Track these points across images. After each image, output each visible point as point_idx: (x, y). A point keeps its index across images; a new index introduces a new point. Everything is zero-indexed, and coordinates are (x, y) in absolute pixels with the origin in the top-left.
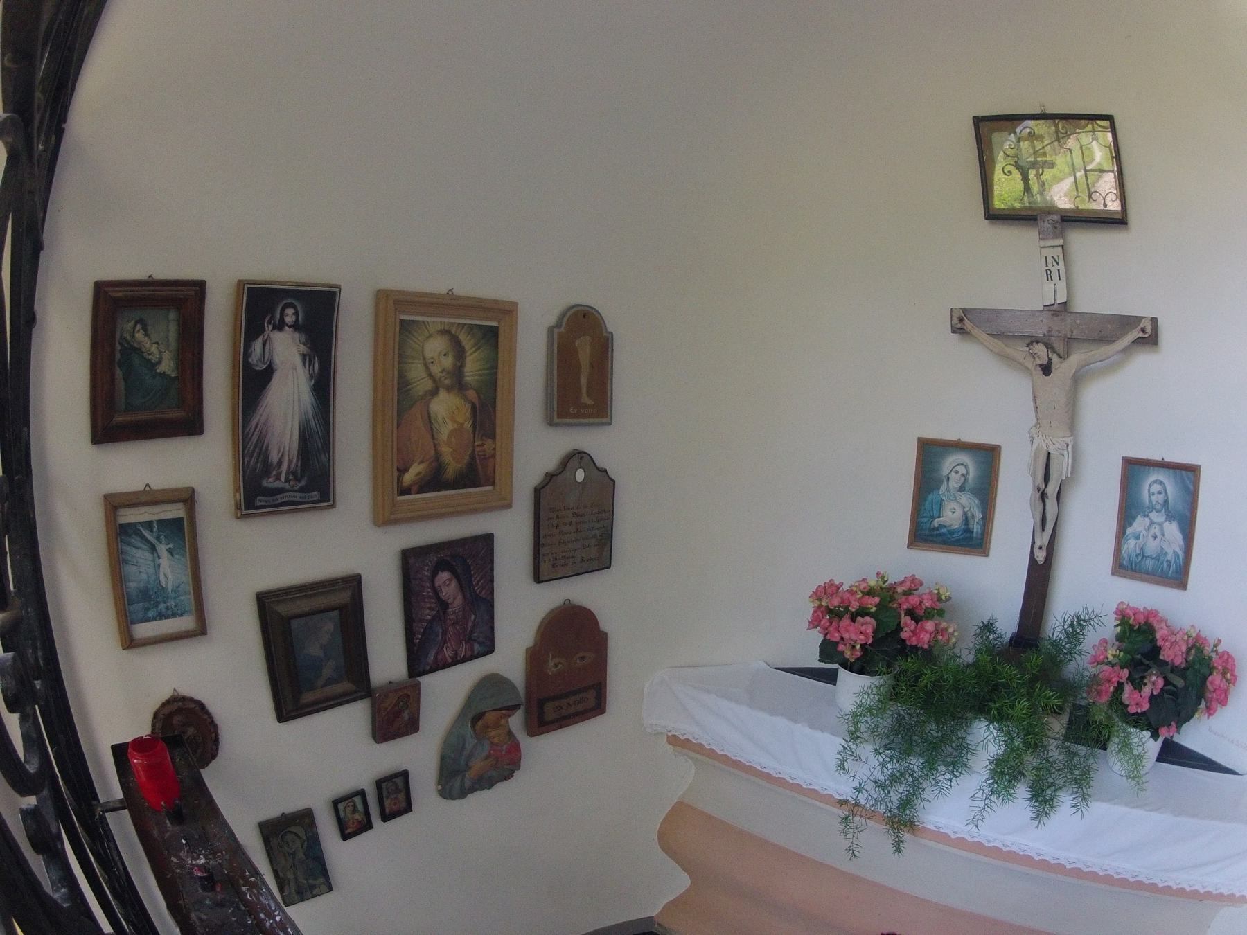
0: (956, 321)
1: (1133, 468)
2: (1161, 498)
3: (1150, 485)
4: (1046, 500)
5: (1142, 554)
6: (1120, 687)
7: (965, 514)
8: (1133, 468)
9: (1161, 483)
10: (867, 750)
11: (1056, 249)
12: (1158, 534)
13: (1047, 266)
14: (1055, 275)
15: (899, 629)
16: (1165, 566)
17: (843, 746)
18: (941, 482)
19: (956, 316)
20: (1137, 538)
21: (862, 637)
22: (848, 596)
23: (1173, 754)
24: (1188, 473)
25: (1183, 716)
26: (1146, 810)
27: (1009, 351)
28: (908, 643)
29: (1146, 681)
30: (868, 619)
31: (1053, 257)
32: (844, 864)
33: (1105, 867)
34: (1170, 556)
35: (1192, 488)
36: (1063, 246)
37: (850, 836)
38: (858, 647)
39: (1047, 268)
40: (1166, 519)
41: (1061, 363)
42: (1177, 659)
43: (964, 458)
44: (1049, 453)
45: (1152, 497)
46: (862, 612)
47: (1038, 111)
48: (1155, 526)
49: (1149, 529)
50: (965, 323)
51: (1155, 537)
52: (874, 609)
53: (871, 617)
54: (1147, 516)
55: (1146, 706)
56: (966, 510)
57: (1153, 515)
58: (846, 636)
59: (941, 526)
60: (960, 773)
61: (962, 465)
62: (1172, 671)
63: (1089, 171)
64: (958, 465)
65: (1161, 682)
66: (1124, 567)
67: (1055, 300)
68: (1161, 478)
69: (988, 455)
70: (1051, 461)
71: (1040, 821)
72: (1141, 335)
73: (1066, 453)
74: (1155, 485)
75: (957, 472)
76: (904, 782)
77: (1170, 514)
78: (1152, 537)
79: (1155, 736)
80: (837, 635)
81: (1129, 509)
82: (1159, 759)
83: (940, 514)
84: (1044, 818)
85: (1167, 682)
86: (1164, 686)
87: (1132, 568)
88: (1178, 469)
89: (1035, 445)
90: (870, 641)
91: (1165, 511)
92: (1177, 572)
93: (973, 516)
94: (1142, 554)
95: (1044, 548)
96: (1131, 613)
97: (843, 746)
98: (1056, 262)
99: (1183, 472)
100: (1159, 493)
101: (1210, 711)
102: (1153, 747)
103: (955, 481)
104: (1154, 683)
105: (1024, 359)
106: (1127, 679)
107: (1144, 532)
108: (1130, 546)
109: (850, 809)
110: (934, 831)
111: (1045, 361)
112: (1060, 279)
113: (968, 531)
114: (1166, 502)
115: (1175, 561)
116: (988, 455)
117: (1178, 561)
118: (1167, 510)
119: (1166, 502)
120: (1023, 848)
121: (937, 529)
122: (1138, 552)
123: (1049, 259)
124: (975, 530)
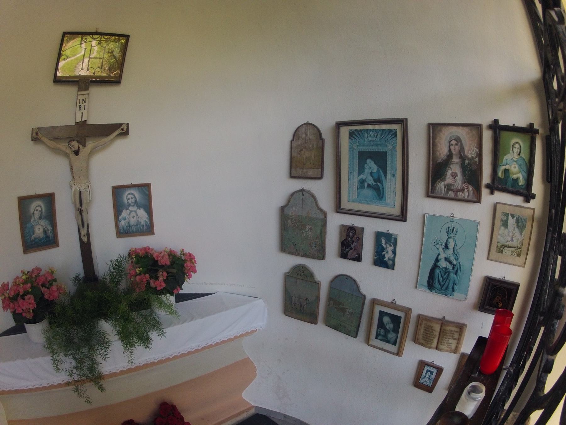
0: (34, 134)
1: (118, 191)
2: (133, 200)
3: (127, 196)
4: (83, 213)
5: (129, 225)
6: (148, 283)
7: (44, 229)
8: (118, 191)
9: (132, 194)
10: (61, 357)
11: (85, 96)
12: (135, 215)
13: (80, 104)
14: (83, 108)
15: (43, 295)
16: (141, 227)
17: (52, 360)
18: (31, 217)
19: (34, 132)
20: (125, 219)
21: (31, 306)
22: (15, 288)
23: (181, 298)
24: (145, 188)
25: (180, 283)
26: (188, 322)
27: (59, 146)
28: (49, 300)
29: (158, 275)
30: (29, 296)
31: (83, 99)
32: (87, 407)
33: (186, 350)
34: (143, 223)
35: (148, 193)
36: (88, 94)
37: (83, 396)
38: (31, 311)
39: (80, 105)
40: (137, 208)
41: (83, 149)
42: (167, 262)
43: (39, 202)
44: (80, 192)
45: (128, 200)
46: (26, 293)
47: (93, 30)
48: (132, 212)
49: (130, 215)
50: (39, 135)
51: (134, 217)
52: (30, 290)
53: (30, 294)
54: (128, 209)
55: (164, 285)
56: (44, 227)
57: (131, 208)
58: (24, 308)
59: (35, 238)
60: (108, 345)
61: (39, 206)
62: (168, 268)
63: (91, 58)
64: (37, 207)
65: (165, 274)
66: (122, 233)
67: (82, 119)
68: (132, 192)
69: (49, 199)
70: (82, 195)
71: (149, 348)
72: (121, 131)
73: (88, 190)
74: (129, 195)
75: (37, 210)
76: (86, 361)
77: (139, 206)
78: (132, 217)
79: (172, 294)
80: (20, 309)
81: (118, 208)
82: (176, 302)
83: (33, 233)
84: (150, 345)
85: (168, 273)
86: (167, 274)
87: (126, 232)
88: (139, 186)
89: (73, 189)
90: (36, 306)
91: (136, 205)
92: (148, 229)
93: (48, 230)
94: (129, 225)
95: (86, 235)
96: (139, 251)
97: (52, 360)
98: (84, 100)
99: (142, 187)
100: (132, 198)
101: (189, 277)
102: (172, 299)
103: (37, 216)
104: (162, 275)
105: (66, 149)
106: (150, 278)
107: (128, 216)
108: (123, 223)
109: (75, 385)
110: (109, 374)
111: (76, 148)
112: (85, 109)
113: (47, 237)
114: (136, 201)
115: (146, 224)
116: (49, 199)
117: (147, 224)
118: (137, 205)
119: (136, 201)
120: (148, 360)
121: (34, 240)
122: (127, 225)
123: (81, 100)
124: (50, 236)
